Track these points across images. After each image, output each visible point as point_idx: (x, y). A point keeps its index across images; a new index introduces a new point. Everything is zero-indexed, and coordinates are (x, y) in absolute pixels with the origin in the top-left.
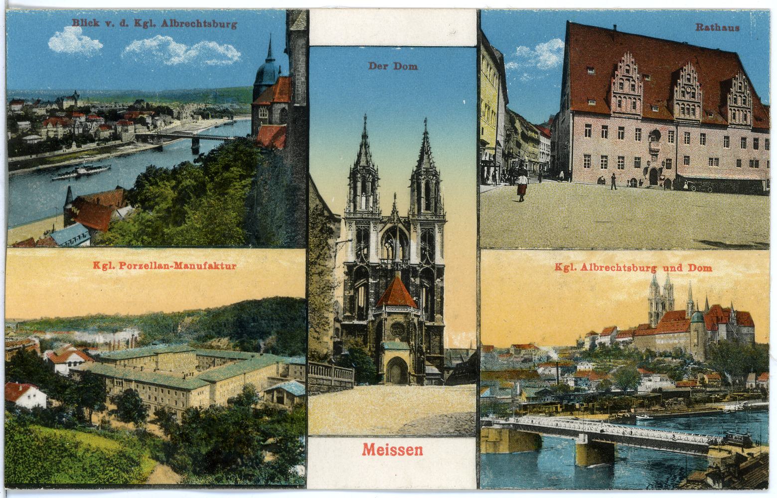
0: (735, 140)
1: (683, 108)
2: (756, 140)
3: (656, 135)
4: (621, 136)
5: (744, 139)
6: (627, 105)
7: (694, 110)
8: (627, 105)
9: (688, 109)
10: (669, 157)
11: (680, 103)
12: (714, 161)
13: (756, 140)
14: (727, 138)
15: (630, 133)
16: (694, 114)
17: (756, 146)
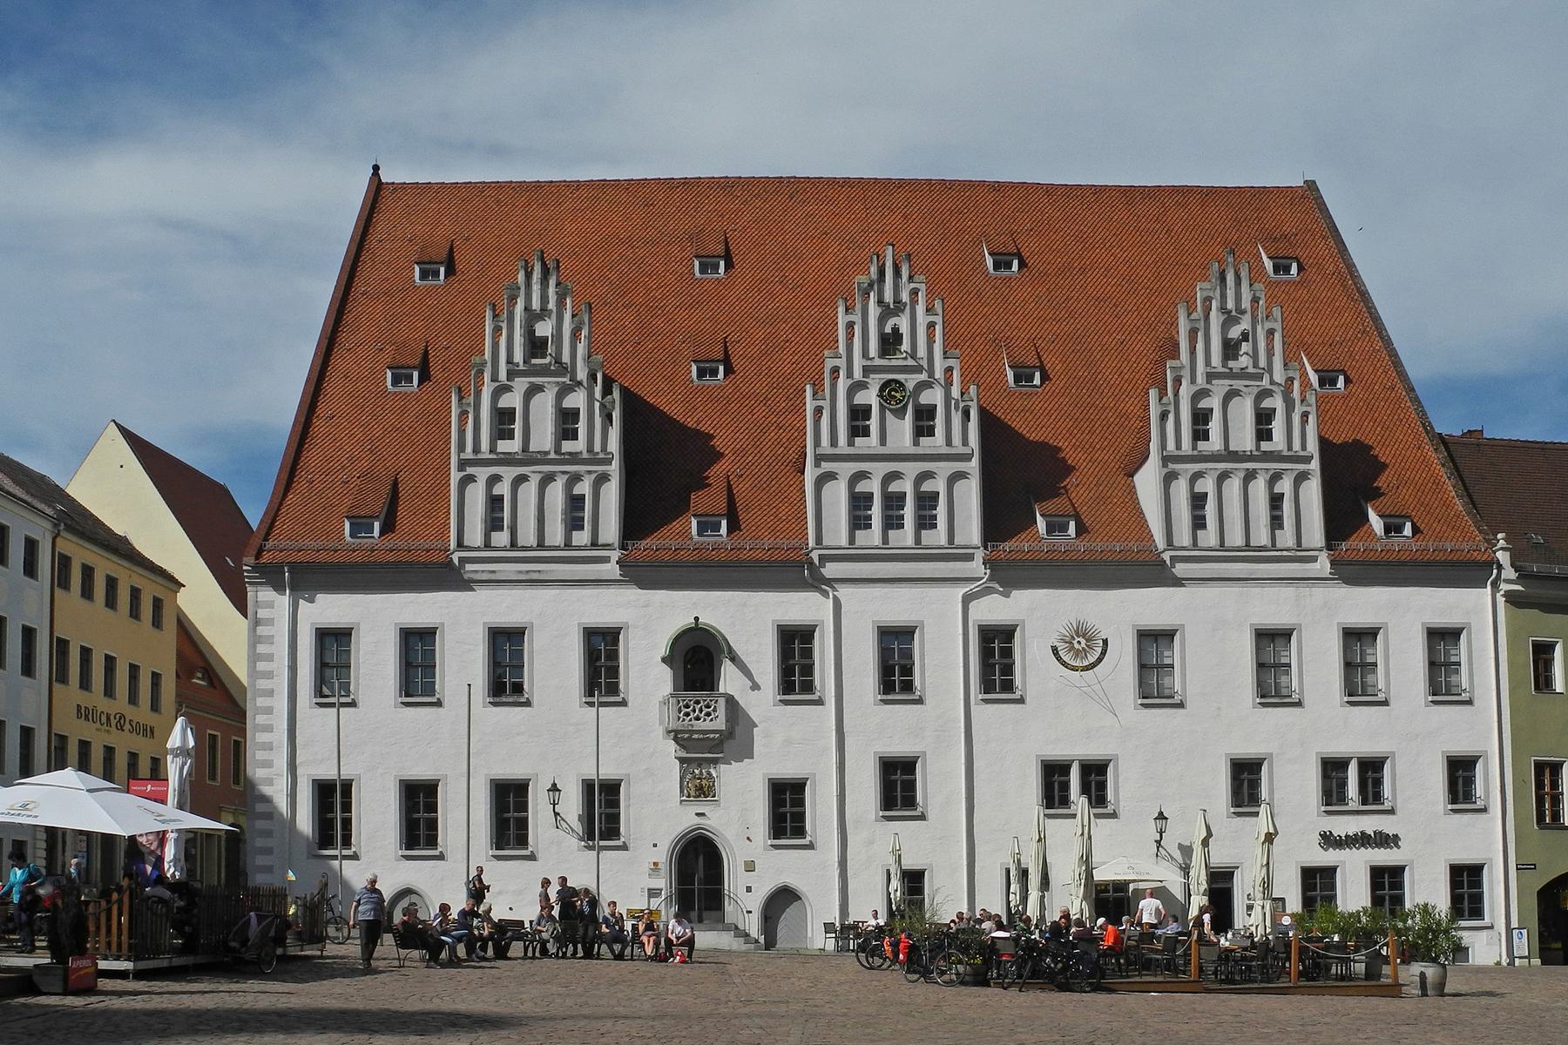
0: (1215, 658)
1: (859, 503)
2: (1358, 640)
3: (697, 659)
4: (506, 680)
5: (1272, 641)
6: (537, 508)
7: (926, 502)
8: (537, 508)
9: (893, 502)
10: (788, 770)
11: (846, 469)
12: (1072, 783)
13: (1358, 640)
14: (1154, 642)
15: (555, 665)
16: (925, 521)
17: (1358, 679)
